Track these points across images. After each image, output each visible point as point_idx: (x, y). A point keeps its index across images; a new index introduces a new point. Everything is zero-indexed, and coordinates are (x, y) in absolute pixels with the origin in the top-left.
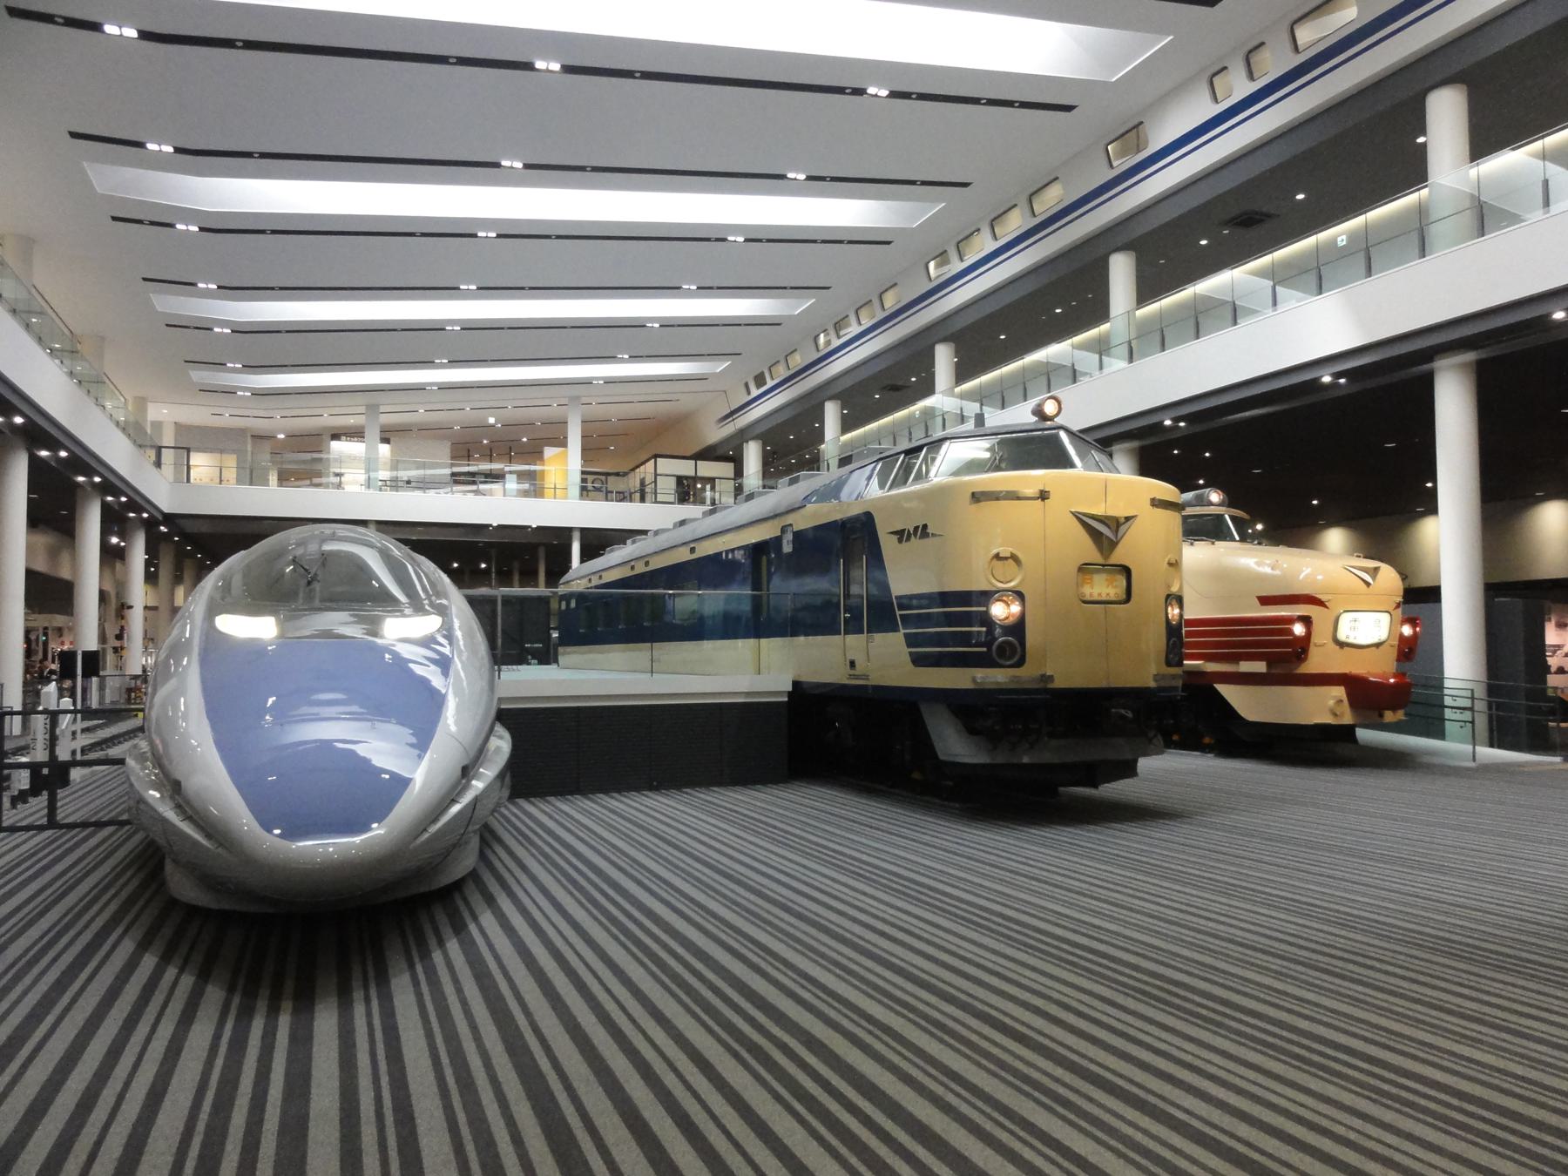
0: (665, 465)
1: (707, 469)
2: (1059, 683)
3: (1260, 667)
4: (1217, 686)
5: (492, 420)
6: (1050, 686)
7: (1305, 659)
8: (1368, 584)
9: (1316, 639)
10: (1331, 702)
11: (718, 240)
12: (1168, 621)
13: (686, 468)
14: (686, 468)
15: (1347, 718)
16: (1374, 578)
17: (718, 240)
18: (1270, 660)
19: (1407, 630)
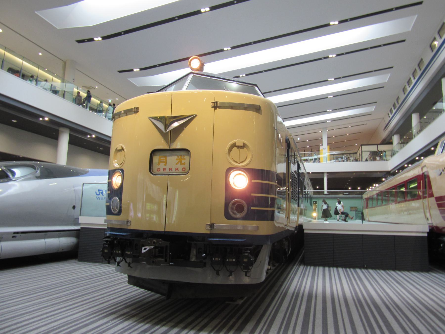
0: (364, 148)
1: (382, 148)
2: (133, 227)
5: (299, 139)
6: (129, 228)
11: (325, 58)
14: (374, 148)
17: (325, 58)
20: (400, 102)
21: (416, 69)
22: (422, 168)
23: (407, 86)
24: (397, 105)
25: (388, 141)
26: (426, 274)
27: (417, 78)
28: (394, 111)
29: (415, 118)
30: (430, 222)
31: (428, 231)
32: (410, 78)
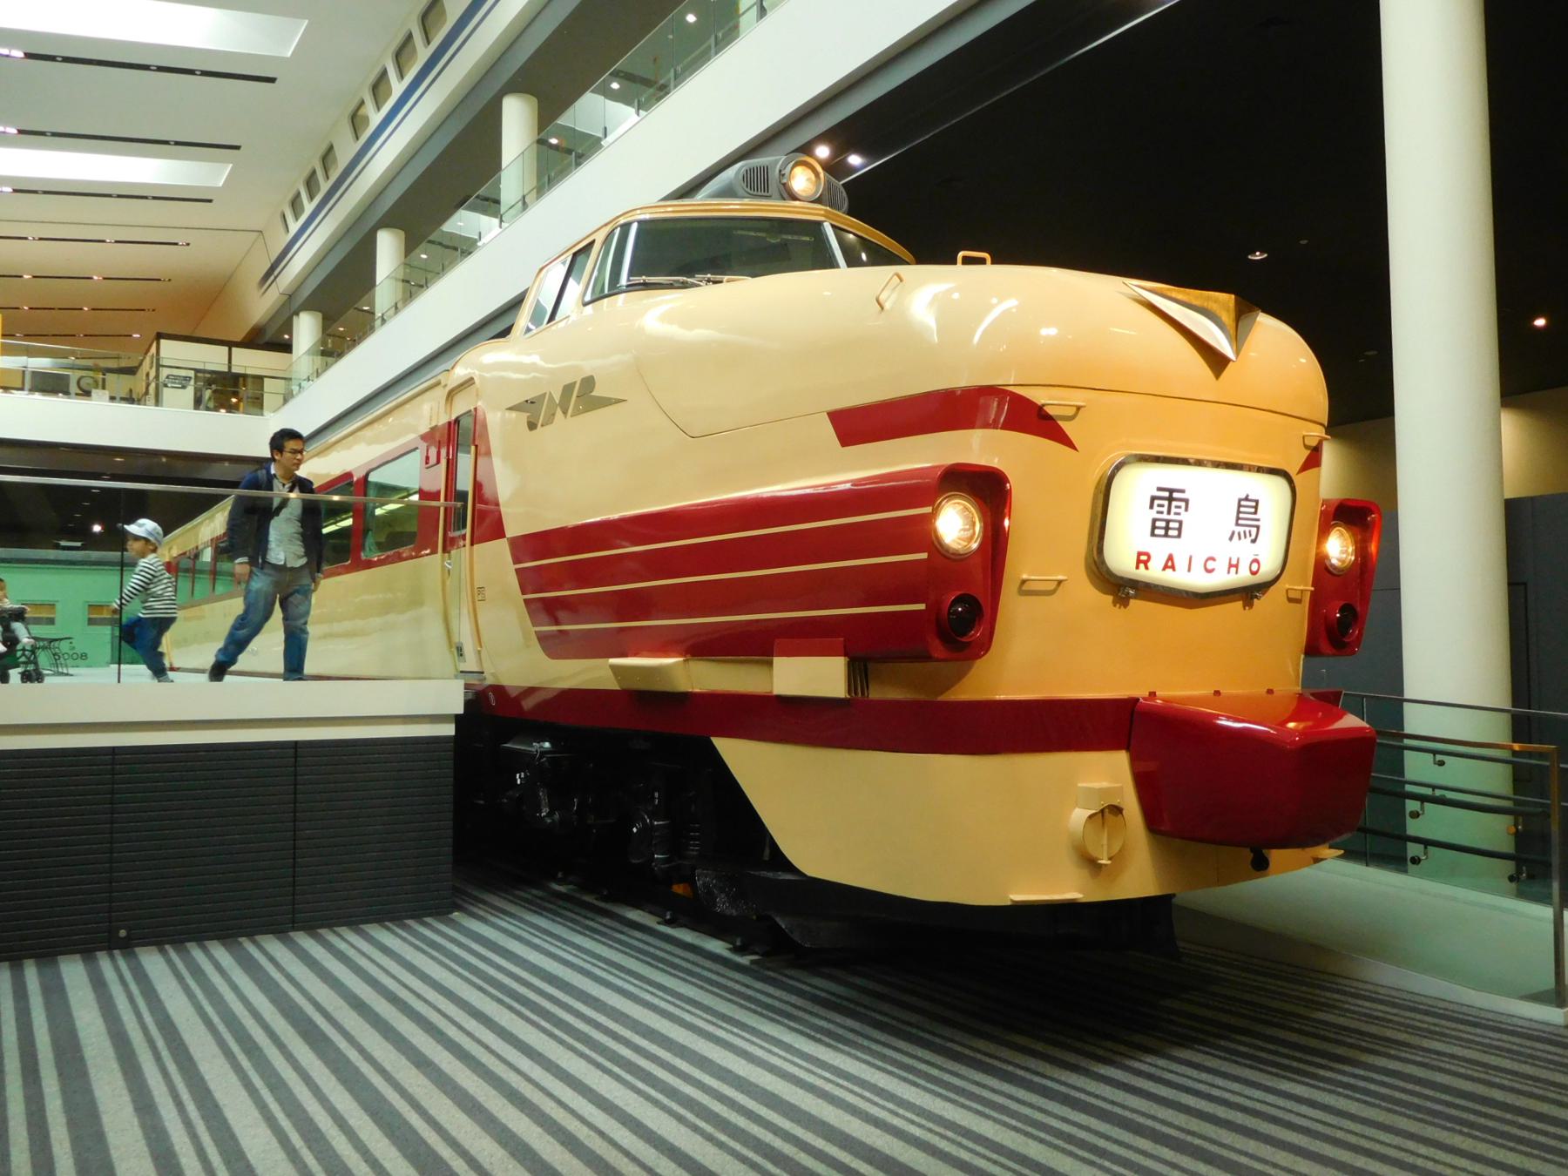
0: (171, 350)
1: (249, 361)
3: (816, 676)
4: (723, 745)
7: (985, 645)
8: (1217, 361)
9: (1025, 563)
10: (1079, 815)
12: (367, 475)
13: (213, 358)
14: (213, 358)
15: (1139, 877)
16: (1238, 339)
18: (865, 649)
19: (1338, 548)
20: (335, 175)
21: (410, 37)
22: (451, 395)
23: (369, 107)
24: (324, 177)
25: (273, 338)
26: (434, 931)
27: (410, 77)
28: (309, 207)
29: (388, 246)
30: (470, 664)
31: (460, 710)
32: (384, 73)
